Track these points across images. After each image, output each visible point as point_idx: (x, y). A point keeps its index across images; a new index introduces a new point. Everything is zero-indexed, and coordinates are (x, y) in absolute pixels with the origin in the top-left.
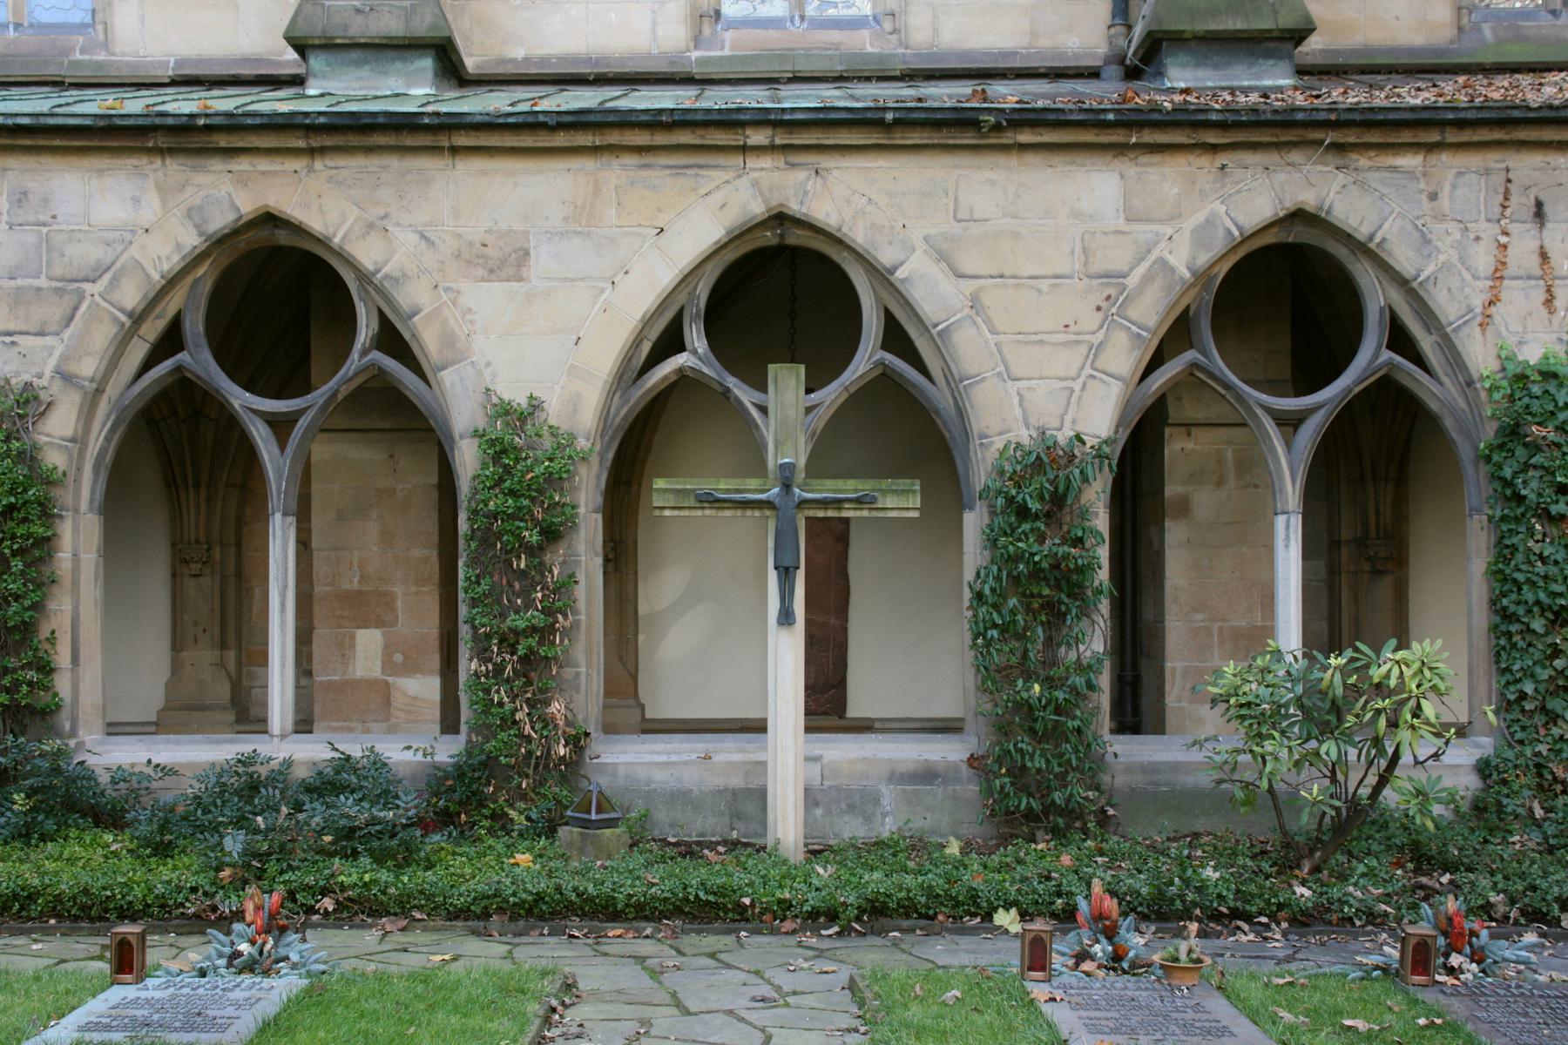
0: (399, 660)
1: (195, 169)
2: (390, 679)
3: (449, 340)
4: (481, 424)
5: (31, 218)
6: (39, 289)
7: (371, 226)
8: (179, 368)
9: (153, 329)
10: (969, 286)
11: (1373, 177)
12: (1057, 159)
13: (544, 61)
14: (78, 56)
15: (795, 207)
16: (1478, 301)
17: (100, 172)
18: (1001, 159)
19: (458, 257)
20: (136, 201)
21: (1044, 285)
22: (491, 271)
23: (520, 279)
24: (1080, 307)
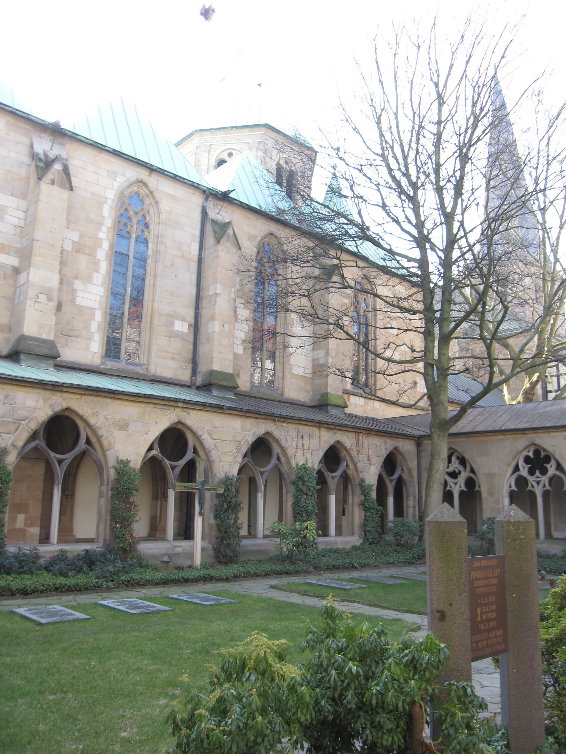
0: (29, 523)
1: (53, 395)
2: (26, 528)
3: (110, 444)
4: (115, 464)
5: (9, 402)
6: (9, 422)
7: (94, 414)
10: (214, 441)
11: (279, 427)
12: (231, 416)
15: (183, 421)
16: (294, 453)
17: (29, 392)
18: (223, 416)
19: (113, 424)
20: (37, 401)
22: (120, 428)
23: (127, 431)
24: (232, 447)
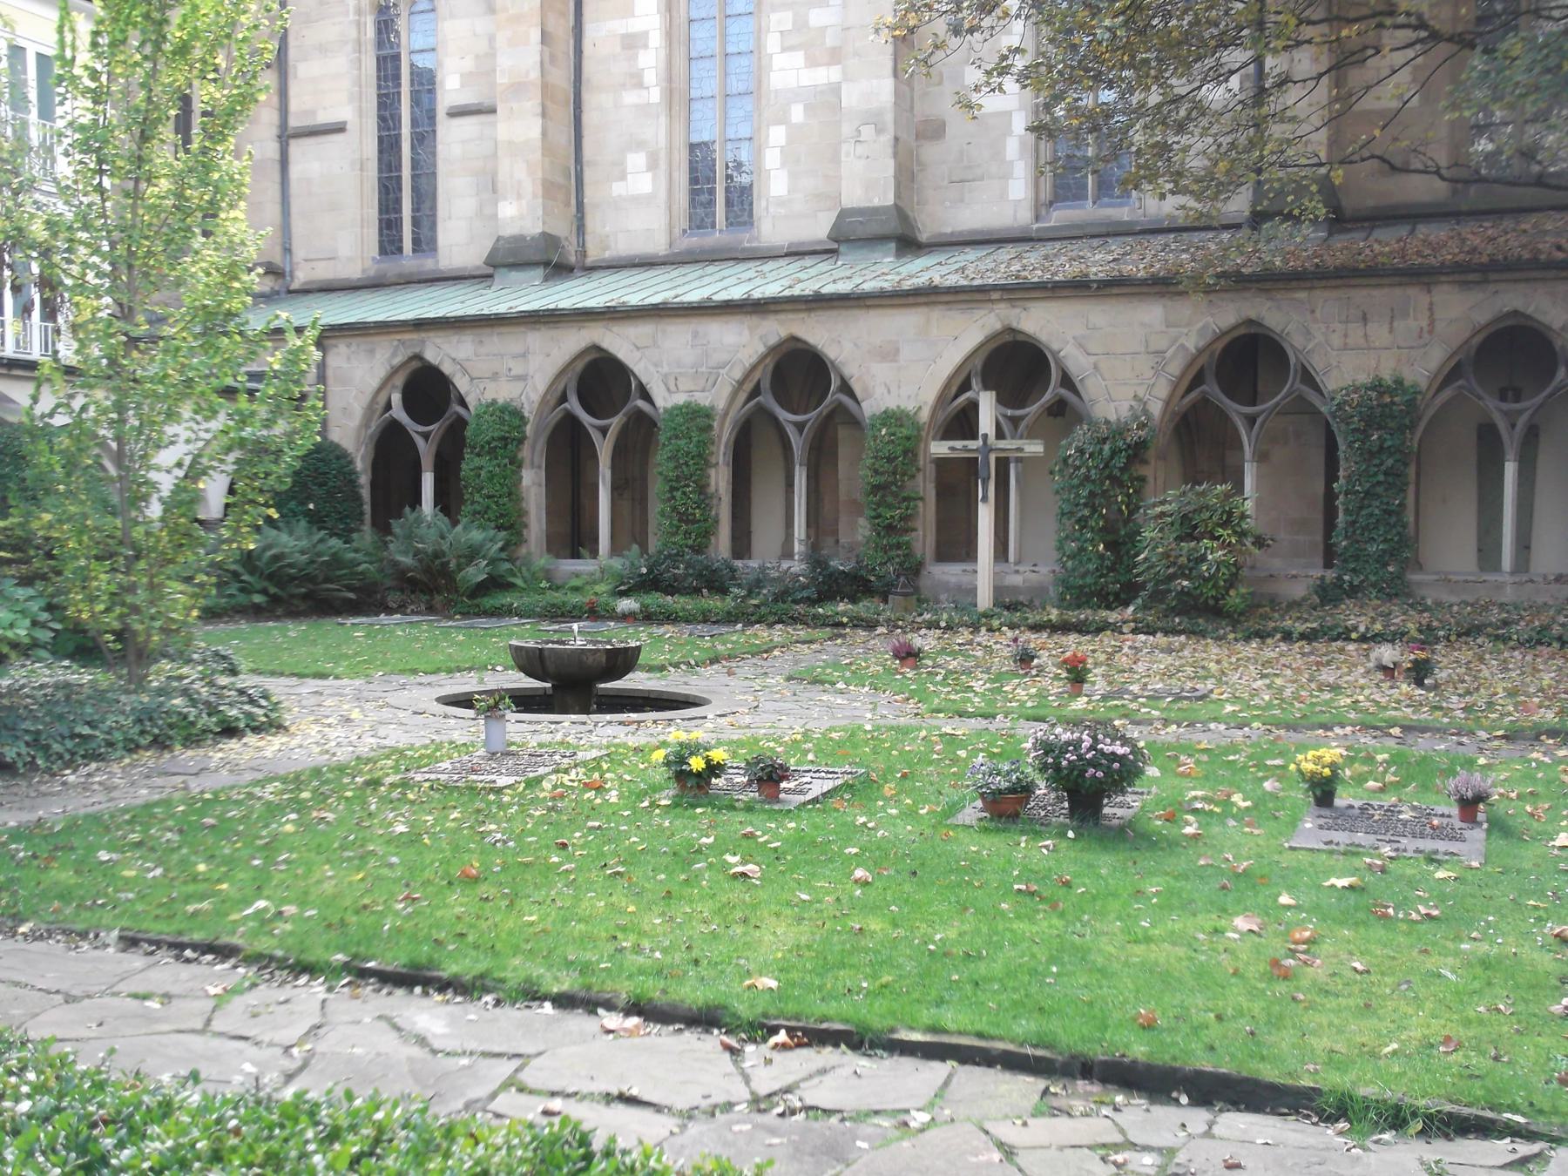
8: (758, 403)
9: (749, 386)
10: (1092, 359)
13: (961, 233)
14: (747, 245)
15: (1014, 325)
21: (1128, 358)
